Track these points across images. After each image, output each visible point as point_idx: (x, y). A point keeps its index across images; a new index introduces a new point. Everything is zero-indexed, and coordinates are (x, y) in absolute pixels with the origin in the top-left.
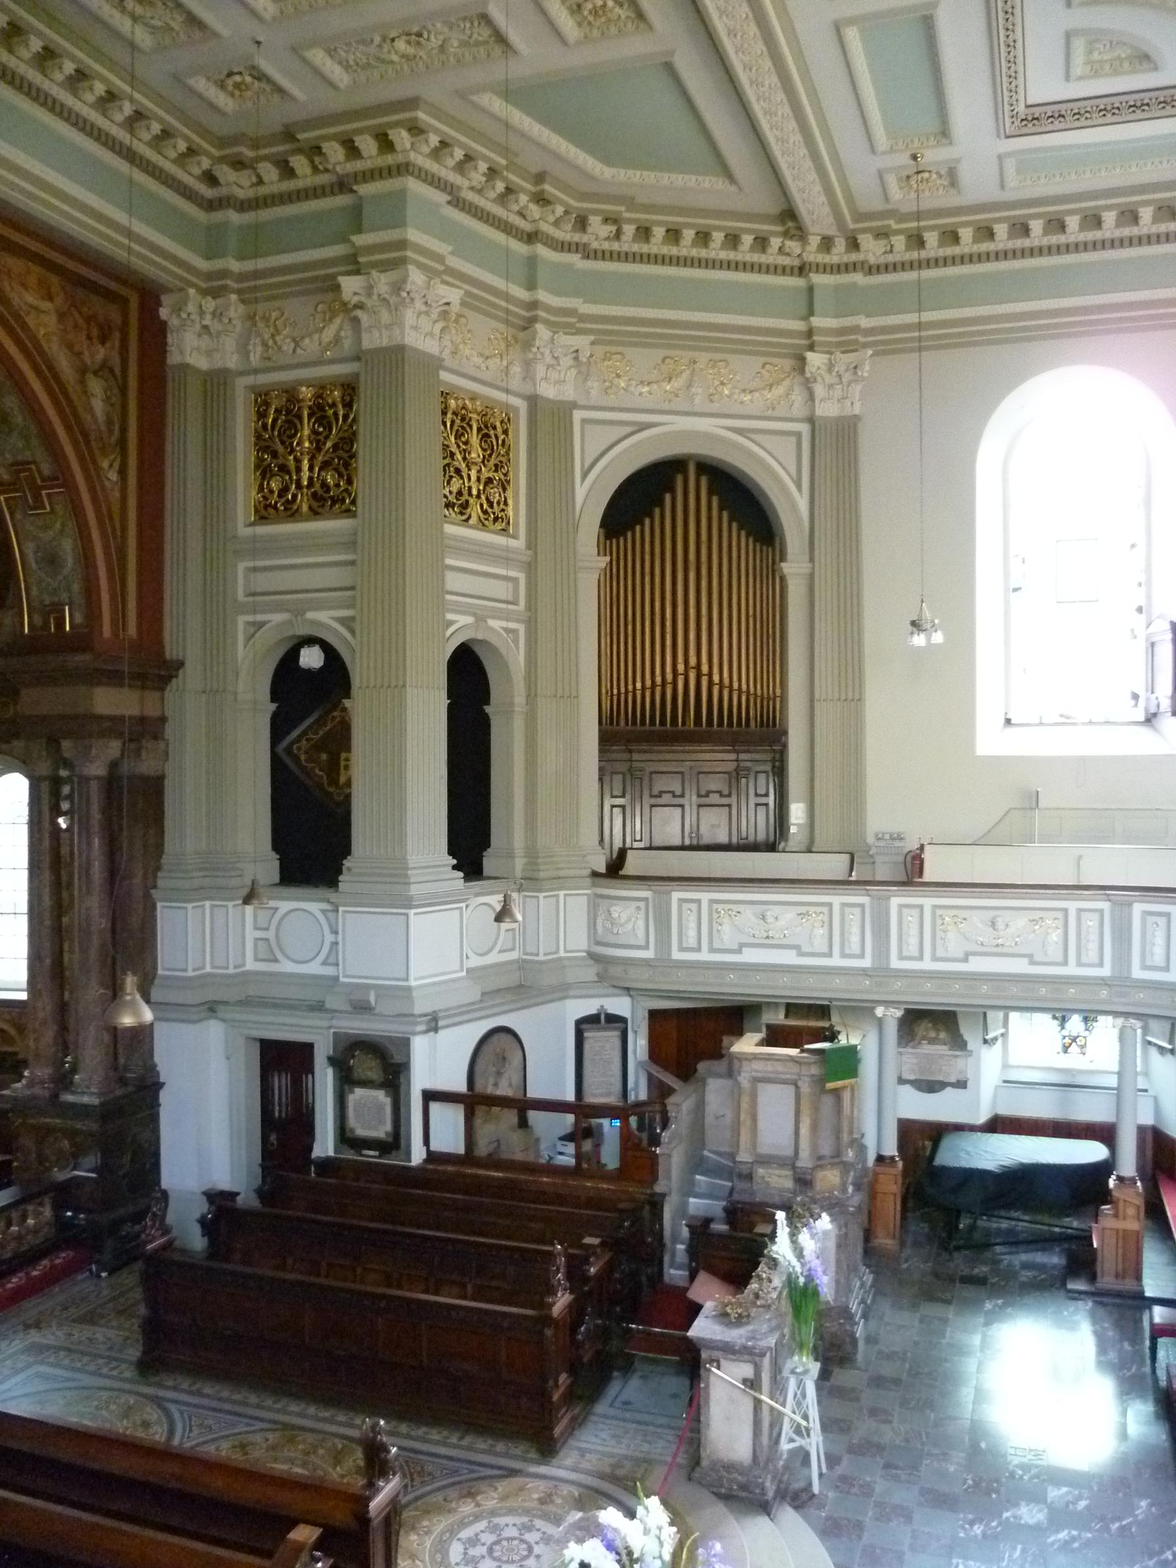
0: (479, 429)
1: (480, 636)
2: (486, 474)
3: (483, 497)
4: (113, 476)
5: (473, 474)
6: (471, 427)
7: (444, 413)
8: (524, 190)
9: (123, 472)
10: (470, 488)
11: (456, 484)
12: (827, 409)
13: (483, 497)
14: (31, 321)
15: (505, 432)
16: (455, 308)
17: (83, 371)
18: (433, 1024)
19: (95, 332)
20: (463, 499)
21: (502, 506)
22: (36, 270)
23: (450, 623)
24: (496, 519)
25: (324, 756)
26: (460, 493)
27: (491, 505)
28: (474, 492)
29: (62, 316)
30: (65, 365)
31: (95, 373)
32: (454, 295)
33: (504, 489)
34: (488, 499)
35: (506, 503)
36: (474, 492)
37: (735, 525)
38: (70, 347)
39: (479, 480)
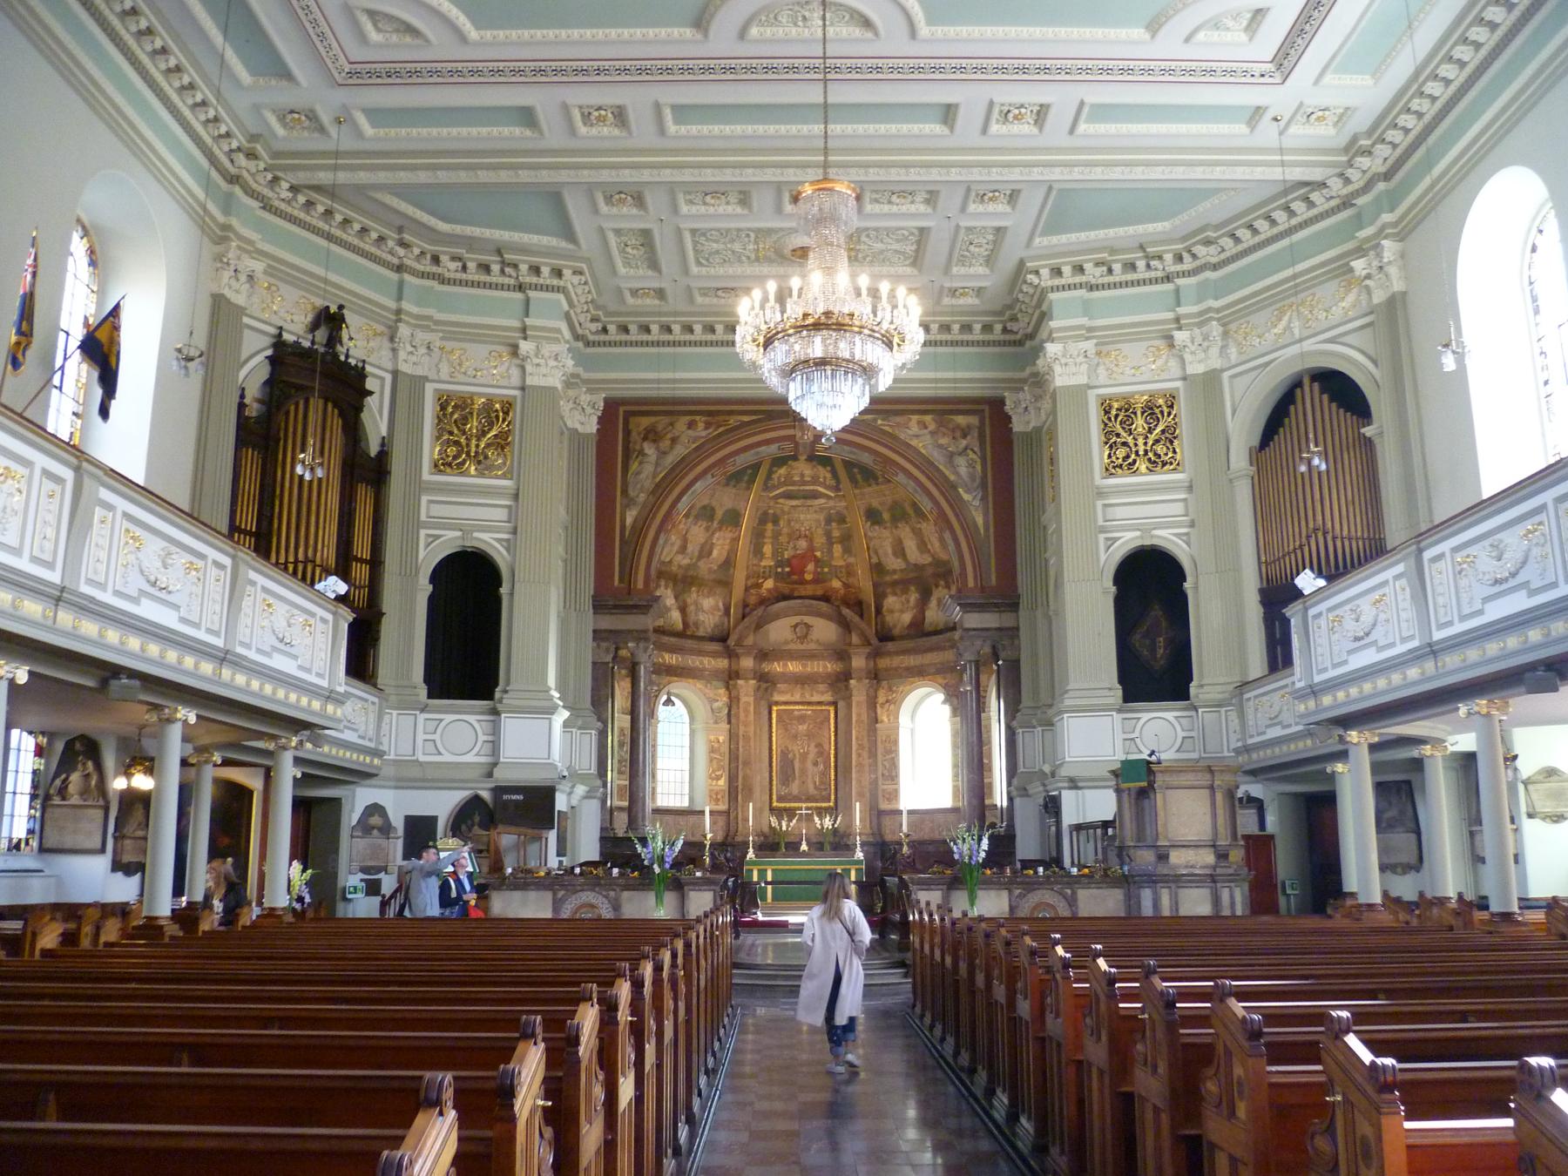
0: (1143, 413)
1: (1148, 542)
2: (1152, 438)
3: (1151, 455)
4: (976, 503)
5: (1141, 441)
6: (1135, 413)
7: (1107, 412)
8: (1139, 258)
9: (984, 499)
10: (1137, 453)
11: (1121, 453)
12: (1379, 297)
13: (1151, 455)
14: (914, 442)
15: (1171, 406)
16: (1092, 351)
17: (951, 455)
18: (1074, 784)
19: (958, 434)
20: (1130, 460)
21: (1170, 455)
22: (915, 418)
23: (1115, 540)
24: (1164, 464)
25: (1147, 642)
26: (1128, 456)
27: (1159, 456)
28: (1141, 453)
29: (932, 433)
30: (938, 458)
31: (960, 454)
32: (1089, 345)
33: (1172, 442)
34: (1156, 454)
35: (1175, 452)
36: (1141, 453)
37: (1342, 411)
38: (940, 446)
39: (1146, 444)
